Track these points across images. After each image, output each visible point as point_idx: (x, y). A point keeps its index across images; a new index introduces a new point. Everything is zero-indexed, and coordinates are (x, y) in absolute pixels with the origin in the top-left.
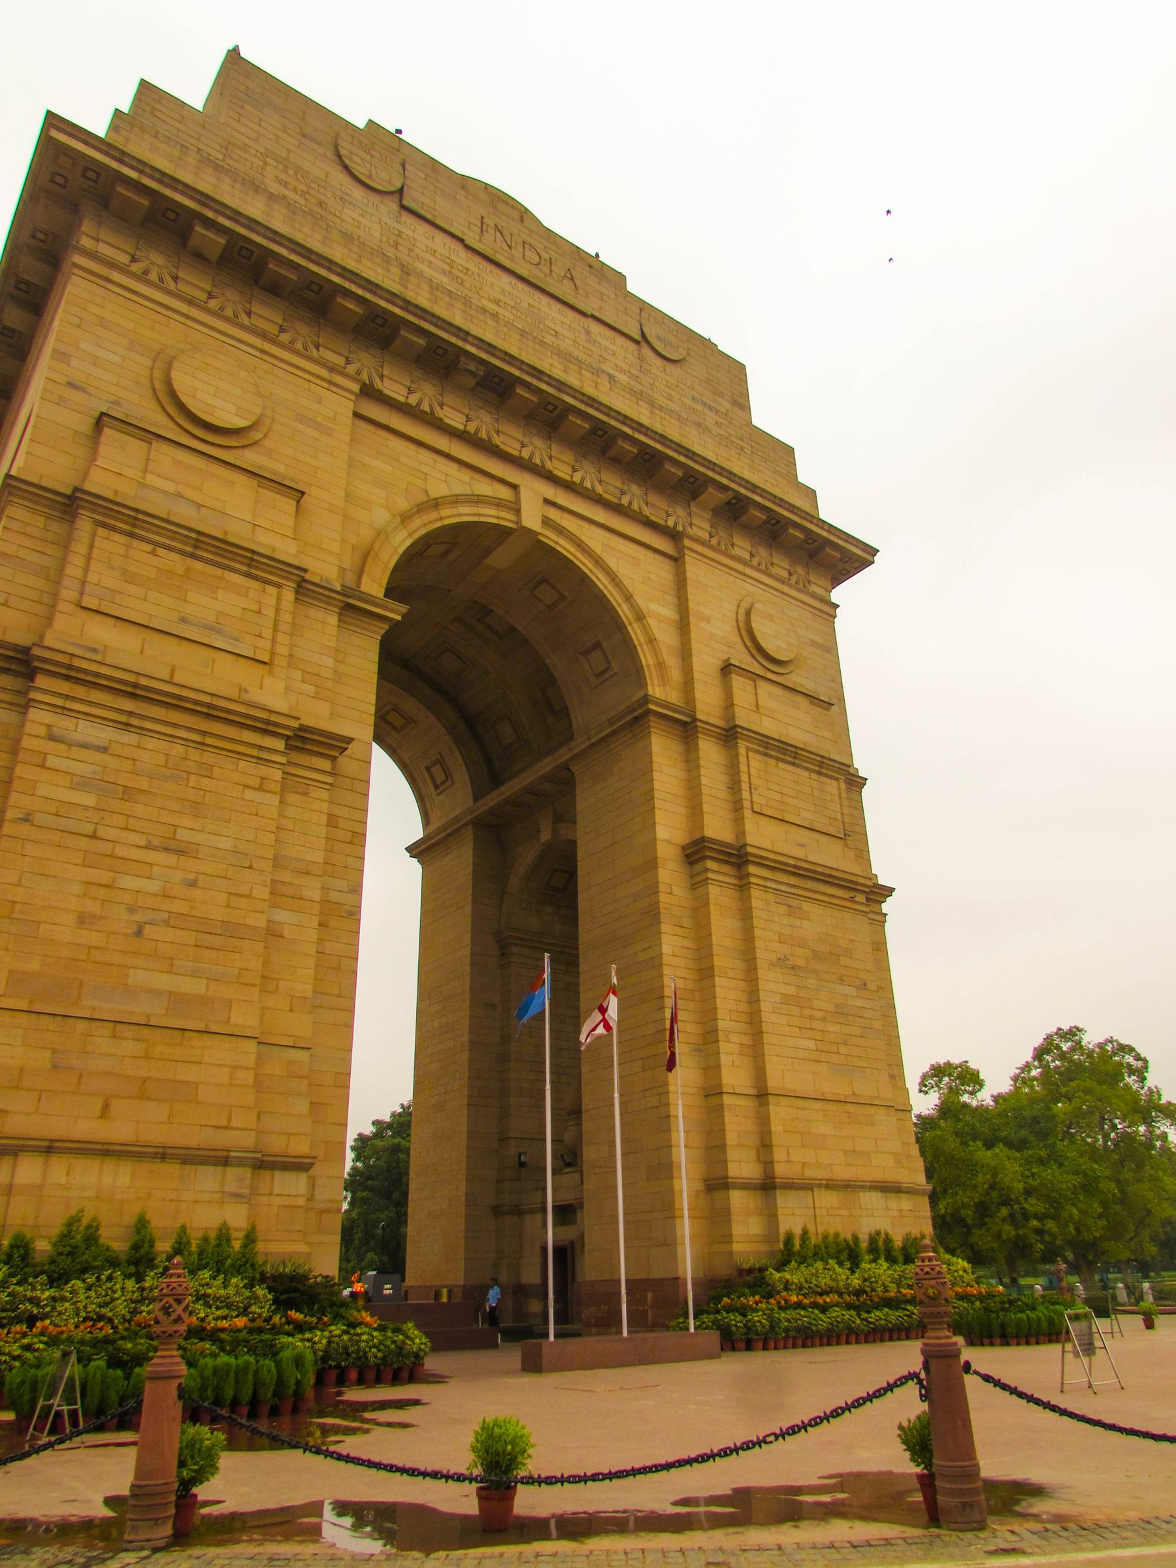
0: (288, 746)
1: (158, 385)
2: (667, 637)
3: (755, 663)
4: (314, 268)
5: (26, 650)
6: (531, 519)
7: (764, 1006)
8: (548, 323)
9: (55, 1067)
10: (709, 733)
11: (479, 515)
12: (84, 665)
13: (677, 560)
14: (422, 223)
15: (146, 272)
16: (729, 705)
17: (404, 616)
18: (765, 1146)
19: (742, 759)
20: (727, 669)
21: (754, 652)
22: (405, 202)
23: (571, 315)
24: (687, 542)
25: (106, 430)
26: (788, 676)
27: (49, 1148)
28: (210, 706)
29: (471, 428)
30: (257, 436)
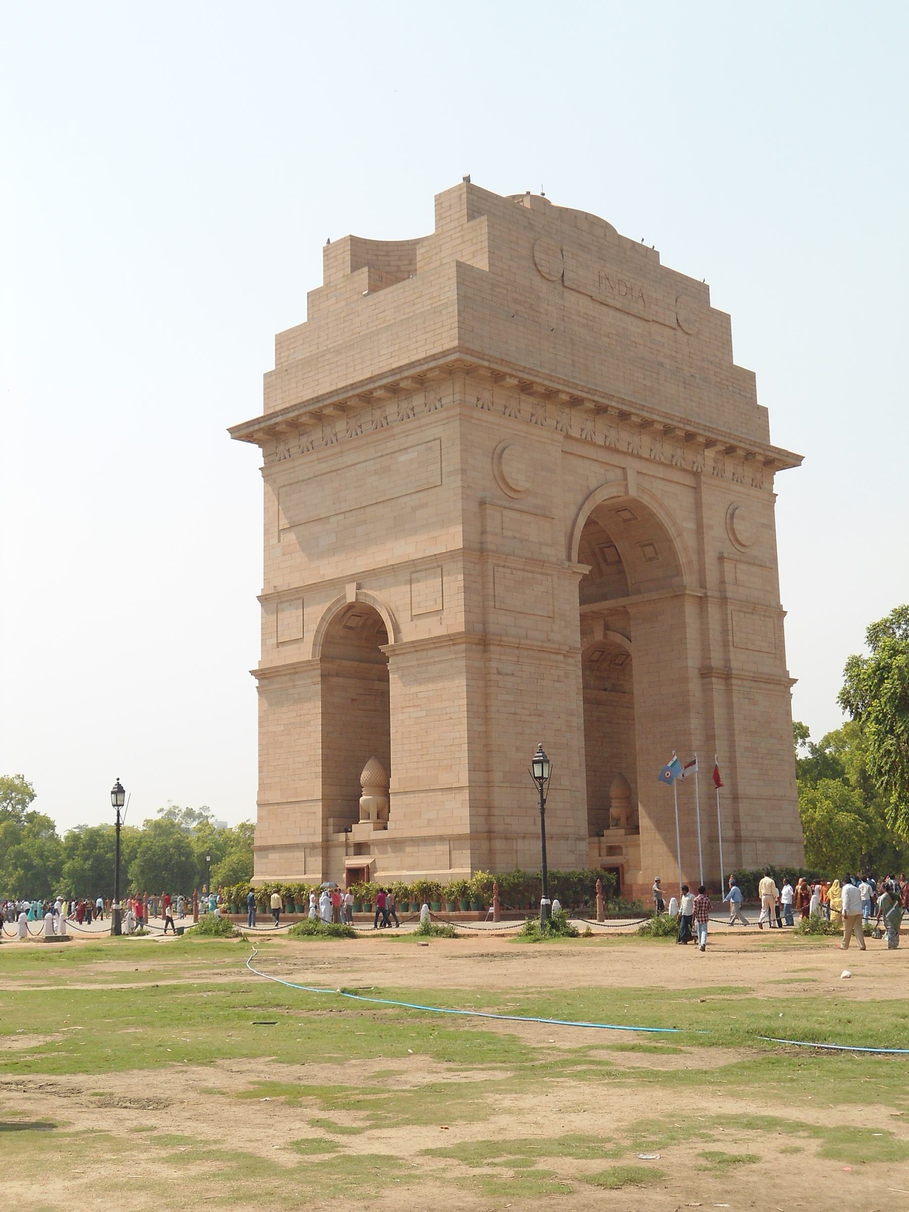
0: (565, 656)
1: (496, 473)
2: (691, 541)
7: (738, 754)
8: (632, 338)
9: (519, 807)
13: (697, 489)
14: (573, 292)
16: (722, 582)
17: (590, 571)
18: (736, 821)
19: (729, 617)
20: (721, 559)
23: (642, 323)
24: (703, 479)
27: (524, 838)
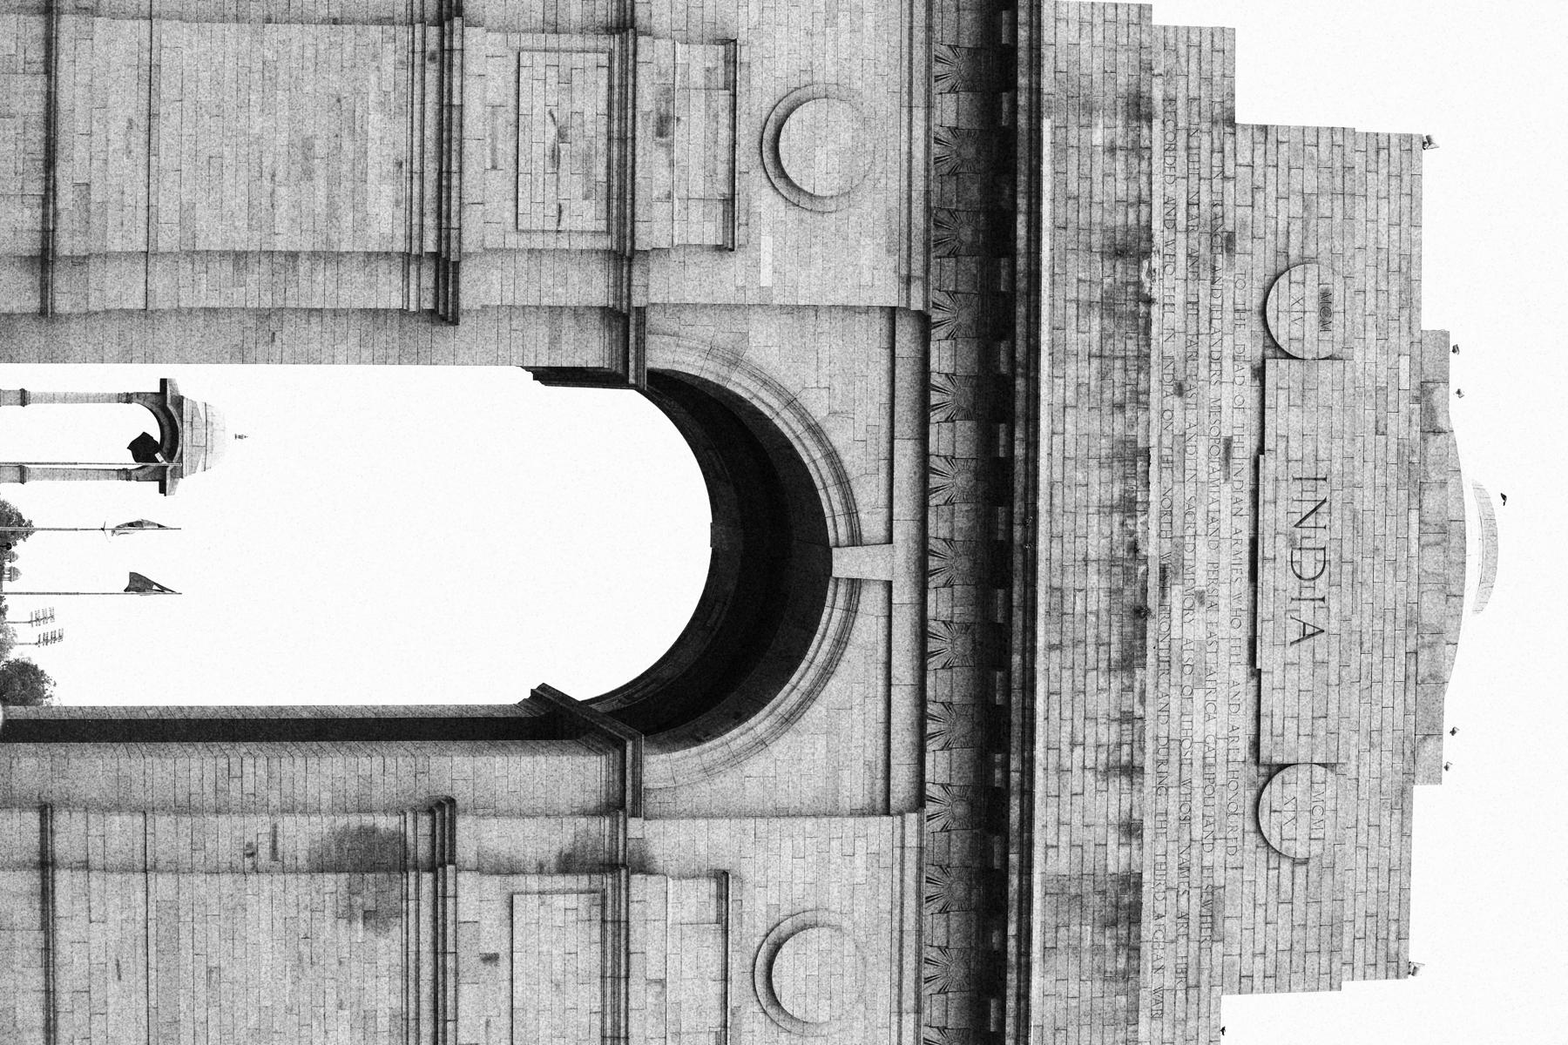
3: (758, 940)
4: (1021, 219)
5: (460, 11)
6: (845, 563)
10: (614, 837)
11: (825, 488)
12: (456, 60)
13: (887, 812)
14: (1255, 395)
15: (938, 60)
18: (86, 866)
20: (722, 878)
21: (773, 936)
22: (1270, 364)
24: (912, 818)
25: (721, 48)
26: (756, 1008)
28: (449, 172)
29: (935, 462)
30: (793, 197)
